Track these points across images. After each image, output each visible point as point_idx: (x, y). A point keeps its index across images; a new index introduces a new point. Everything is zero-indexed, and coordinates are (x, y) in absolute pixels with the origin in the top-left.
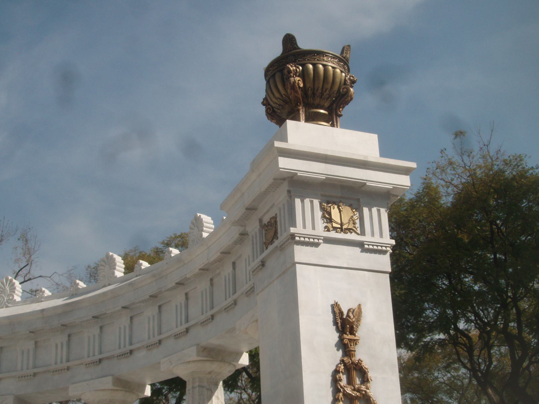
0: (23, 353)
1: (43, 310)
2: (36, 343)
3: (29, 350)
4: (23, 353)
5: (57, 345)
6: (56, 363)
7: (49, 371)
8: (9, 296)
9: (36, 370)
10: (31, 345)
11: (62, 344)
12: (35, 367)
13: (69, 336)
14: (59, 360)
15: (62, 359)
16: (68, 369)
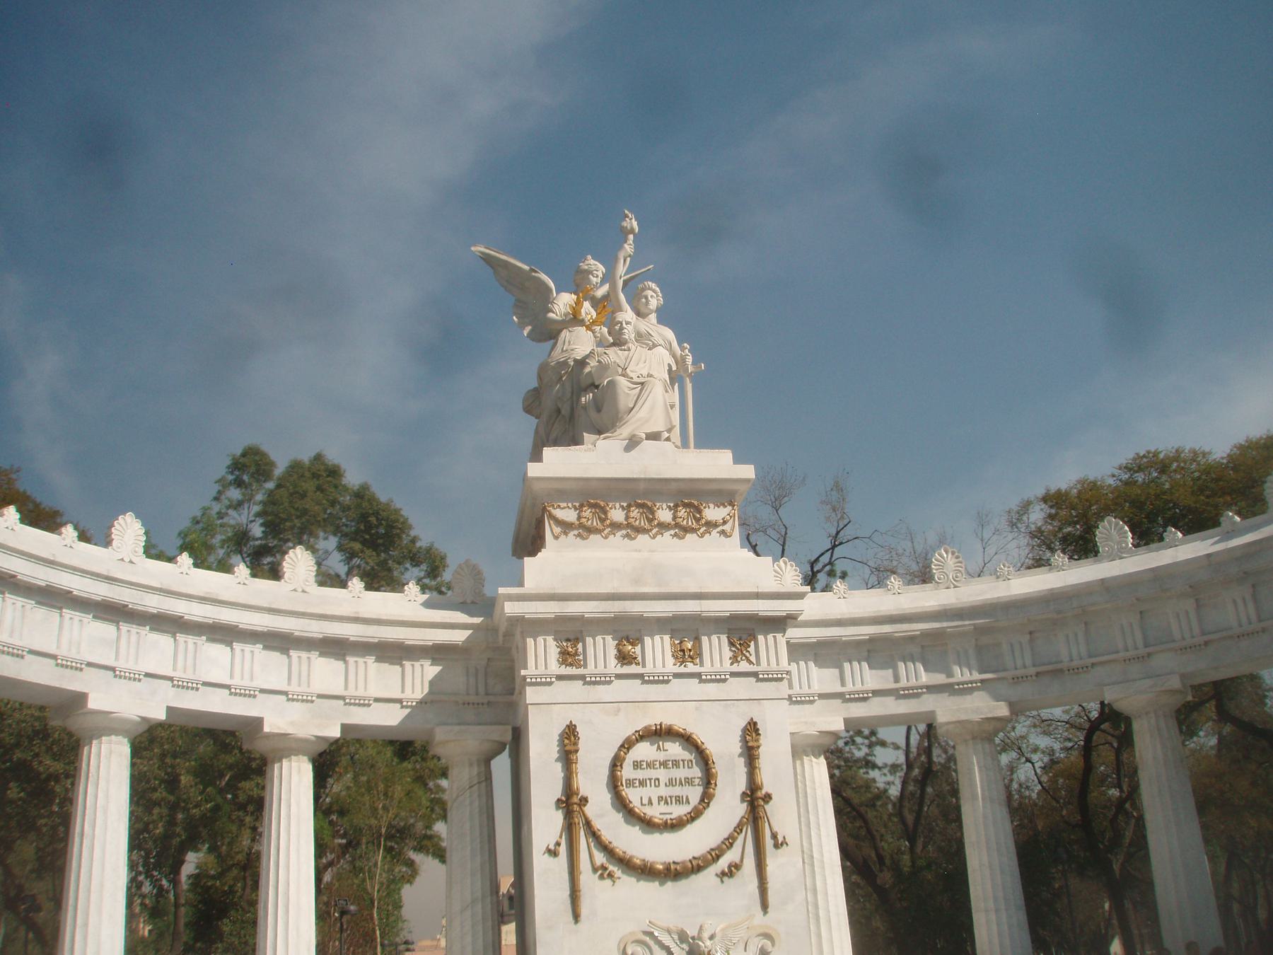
0: (1178, 616)
1: (1209, 556)
2: (1197, 600)
3: (1187, 612)
4: (1178, 616)
5: (1234, 602)
6: (1240, 626)
7: (1231, 637)
8: (1119, 543)
9: (1206, 638)
10: (1189, 605)
11: (1244, 600)
12: (1203, 633)
13: (1254, 586)
14: (1244, 620)
15: (1248, 618)
16: (1264, 630)
